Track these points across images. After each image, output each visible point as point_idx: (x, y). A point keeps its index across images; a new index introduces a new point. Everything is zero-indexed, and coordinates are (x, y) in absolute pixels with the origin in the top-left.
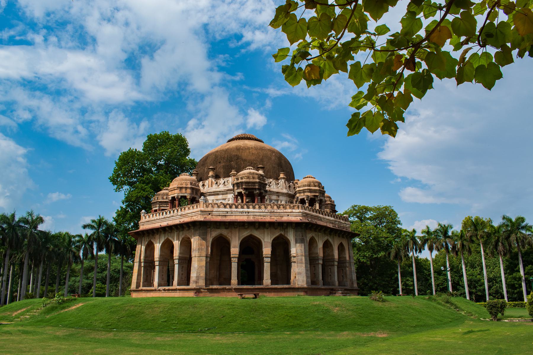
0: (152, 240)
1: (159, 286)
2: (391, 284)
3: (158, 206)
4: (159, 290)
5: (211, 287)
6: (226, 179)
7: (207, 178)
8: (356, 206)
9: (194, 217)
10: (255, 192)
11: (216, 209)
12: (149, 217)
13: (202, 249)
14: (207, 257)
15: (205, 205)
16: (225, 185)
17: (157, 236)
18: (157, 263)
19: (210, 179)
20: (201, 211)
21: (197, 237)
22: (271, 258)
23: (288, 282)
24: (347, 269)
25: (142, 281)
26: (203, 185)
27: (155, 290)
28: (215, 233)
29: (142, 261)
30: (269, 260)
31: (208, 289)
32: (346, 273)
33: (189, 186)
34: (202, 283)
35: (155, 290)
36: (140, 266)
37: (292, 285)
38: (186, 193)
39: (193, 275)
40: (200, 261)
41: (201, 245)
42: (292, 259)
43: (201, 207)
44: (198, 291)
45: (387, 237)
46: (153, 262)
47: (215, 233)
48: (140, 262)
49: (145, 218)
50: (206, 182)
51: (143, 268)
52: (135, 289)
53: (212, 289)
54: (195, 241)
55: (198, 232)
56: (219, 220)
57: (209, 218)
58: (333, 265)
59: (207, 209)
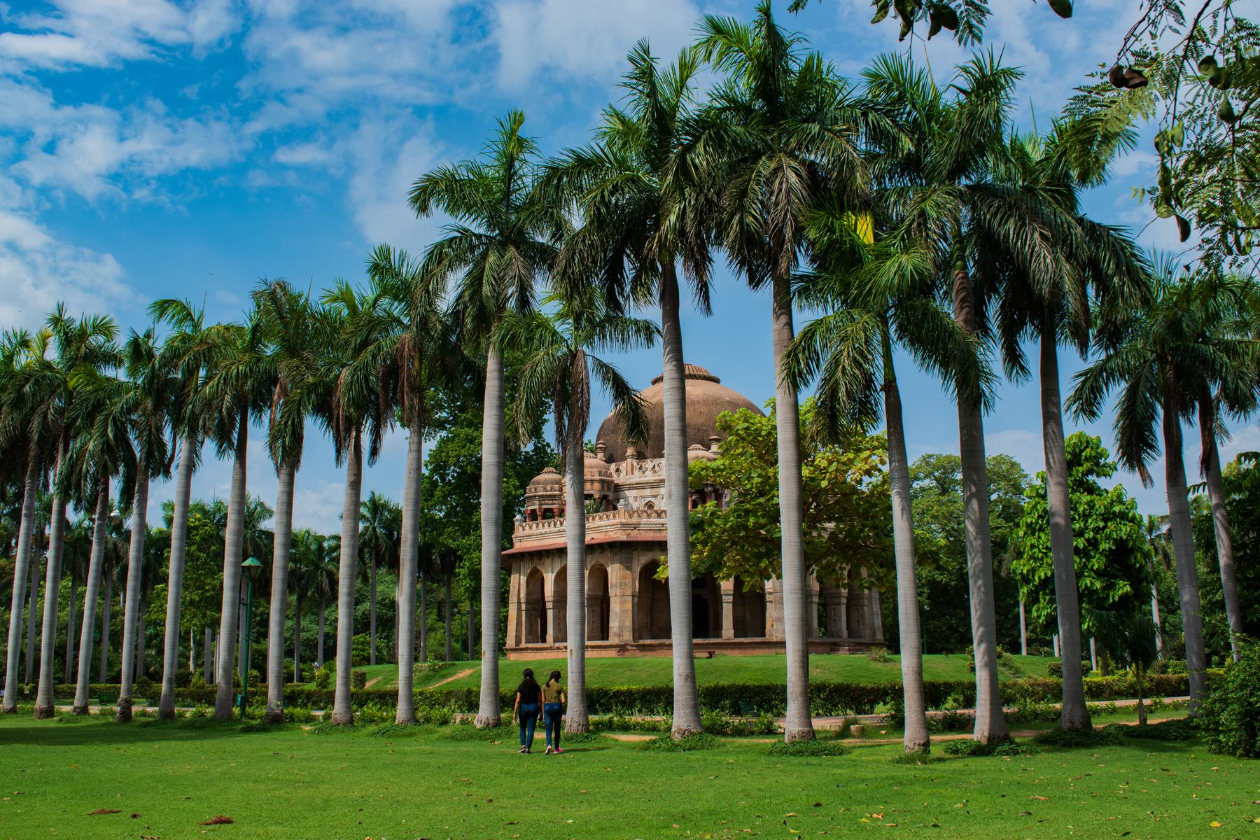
0: (539, 567)
1: (555, 641)
2: (1007, 629)
3: (537, 502)
4: (558, 648)
5: (642, 642)
6: (657, 461)
7: (624, 458)
8: (930, 456)
9: (611, 533)
10: (706, 490)
11: (644, 520)
12: (531, 528)
13: (626, 585)
14: (633, 596)
15: (627, 515)
16: (655, 472)
17: (548, 561)
18: (549, 605)
19: (629, 460)
20: (622, 524)
21: (617, 565)
22: (733, 595)
23: (763, 635)
24: (866, 608)
25: (524, 633)
26: (617, 470)
27: (551, 648)
28: (644, 559)
29: (523, 600)
30: (730, 599)
31: (637, 646)
32: (863, 616)
33: (597, 477)
34: (628, 637)
35: (551, 648)
36: (519, 609)
37: (767, 638)
38: (592, 489)
39: (614, 624)
40: (622, 603)
41: (625, 578)
42: (767, 596)
43: (620, 517)
44: (622, 648)
45: (997, 528)
46: (544, 603)
47: (644, 559)
48: (519, 603)
49: (523, 529)
50: (623, 466)
51: (524, 613)
52: (514, 647)
53: (644, 646)
54: (615, 572)
55: (618, 557)
56: (651, 539)
57: (636, 536)
58: (839, 604)
59: (630, 521)
